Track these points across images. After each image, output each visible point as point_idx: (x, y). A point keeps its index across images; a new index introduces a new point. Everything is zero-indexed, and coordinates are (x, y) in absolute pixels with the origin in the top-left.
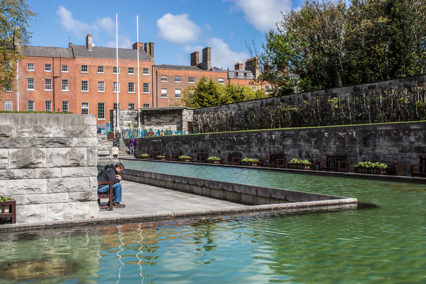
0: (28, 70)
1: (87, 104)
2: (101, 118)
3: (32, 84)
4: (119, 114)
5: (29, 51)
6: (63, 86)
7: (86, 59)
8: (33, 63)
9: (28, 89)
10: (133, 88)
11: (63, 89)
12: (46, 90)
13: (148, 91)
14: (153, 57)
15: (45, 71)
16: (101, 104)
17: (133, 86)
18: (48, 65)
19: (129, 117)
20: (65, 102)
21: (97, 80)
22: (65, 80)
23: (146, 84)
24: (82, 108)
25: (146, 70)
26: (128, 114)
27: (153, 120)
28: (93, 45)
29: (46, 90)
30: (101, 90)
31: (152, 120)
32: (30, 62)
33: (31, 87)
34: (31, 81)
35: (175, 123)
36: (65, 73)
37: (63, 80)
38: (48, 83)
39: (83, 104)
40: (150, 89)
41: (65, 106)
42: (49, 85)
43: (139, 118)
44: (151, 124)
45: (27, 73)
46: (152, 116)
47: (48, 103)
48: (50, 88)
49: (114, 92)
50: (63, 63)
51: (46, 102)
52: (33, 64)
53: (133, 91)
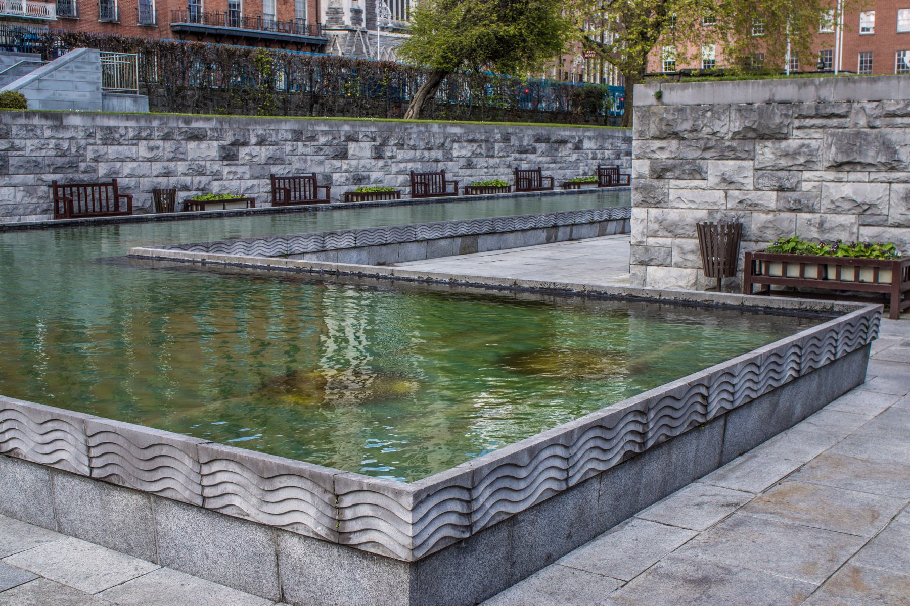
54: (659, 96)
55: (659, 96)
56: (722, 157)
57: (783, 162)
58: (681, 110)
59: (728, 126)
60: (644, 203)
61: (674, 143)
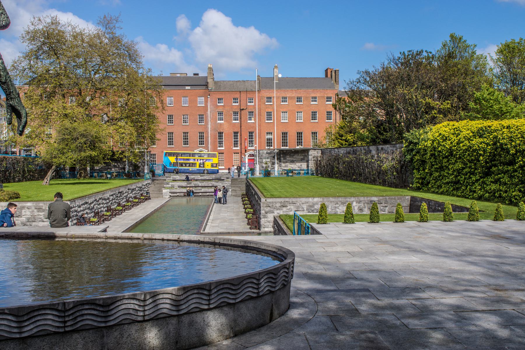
0: (218, 104)
1: (271, 133)
2: (285, 146)
3: (221, 117)
4: (259, 154)
5: (220, 86)
6: (249, 117)
7: (270, 91)
8: (223, 97)
9: (218, 122)
10: (316, 117)
11: (249, 120)
12: (234, 122)
13: (331, 119)
14: (338, 84)
15: (233, 104)
16: (285, 133)
17: (316, 115)
18: (236, 99)
19: (267, 156)
20: (251, 132)
21: (281, 110)
22: (251, 112)
23: (329, 112)
24: (266, 137)
25: (329, 99)
26: (267, 153)
27: (288, 158)
28: (280, 76)
29: (234, 122)
30: (285, 120)
31: (287, 159)
32: (220, 97)
33: (221, 119)
34: (220, 114)
35: (305, 161)
36: (251, 106)
37: (249, 112)
38: (236, 116)
39: (267, 133)
40: (333, 116)
41: (251, 136)
42: (237, 117)
43: (276, 157)
44: (287, 162)
45: (217, 106)
46: (287, 155)
47: (236, 133)
48: (238, 120)
49: (297, 121)
50: (248, 95)
51: (234, 132)
52: (222, 99)
53: (316, 120)
54: (266, 200)
55: (266, 200)
56: (277, 210)
57: (287, 210)
58: (270, 202)
59: (278, 205)
60: (264, 218)
61: (269, 208)
